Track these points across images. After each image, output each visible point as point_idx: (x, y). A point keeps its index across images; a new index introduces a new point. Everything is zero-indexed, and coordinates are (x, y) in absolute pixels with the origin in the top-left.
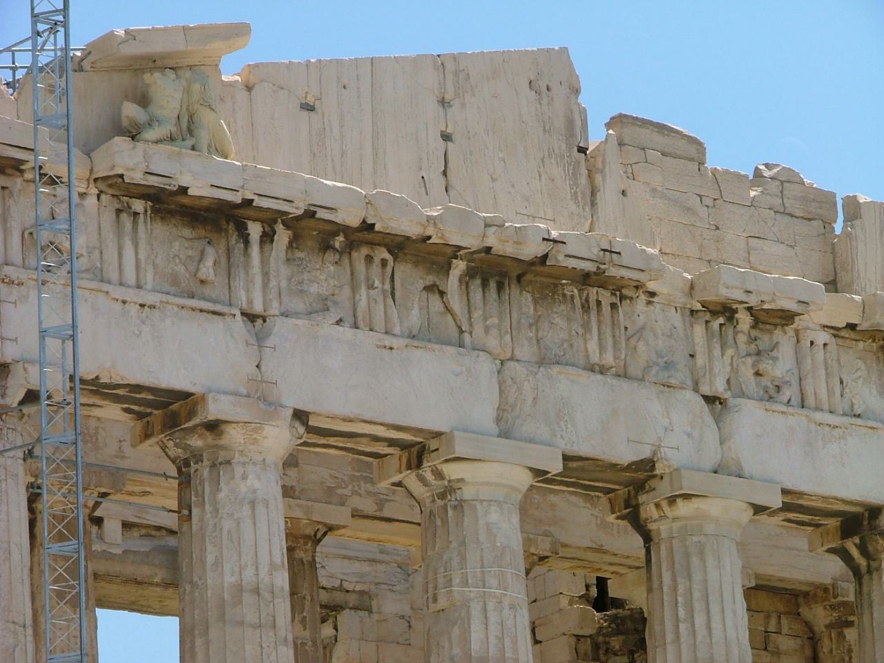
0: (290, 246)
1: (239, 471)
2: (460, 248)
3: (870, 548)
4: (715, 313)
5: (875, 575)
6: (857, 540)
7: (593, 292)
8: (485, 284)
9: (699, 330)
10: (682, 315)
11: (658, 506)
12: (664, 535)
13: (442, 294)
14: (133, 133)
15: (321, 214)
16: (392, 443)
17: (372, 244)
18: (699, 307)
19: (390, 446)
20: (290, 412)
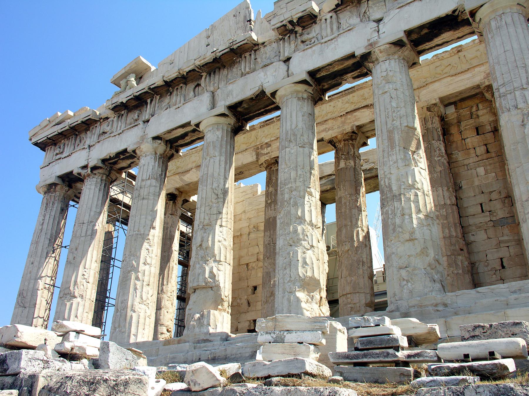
2: (194, 70)
4: (285, 35)
15: (152, 87)
18: (281, 37)
20: (151, 139)
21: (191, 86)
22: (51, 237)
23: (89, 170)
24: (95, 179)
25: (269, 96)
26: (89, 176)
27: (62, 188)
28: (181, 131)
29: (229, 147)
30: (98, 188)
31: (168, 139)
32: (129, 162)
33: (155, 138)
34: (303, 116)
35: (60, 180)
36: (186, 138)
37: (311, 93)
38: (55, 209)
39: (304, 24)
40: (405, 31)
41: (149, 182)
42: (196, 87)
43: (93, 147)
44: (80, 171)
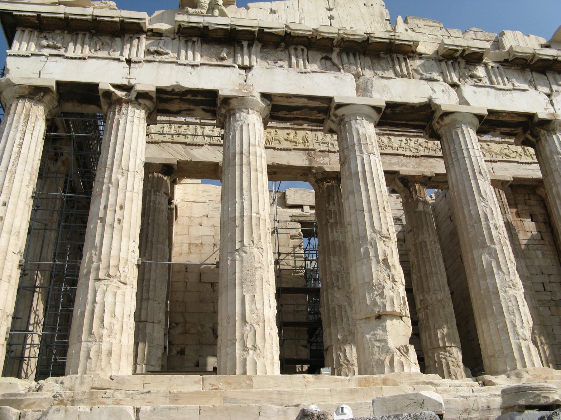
0: (263, 48)
1: (238, 115)
2: (332, 39)
3: (535, 133)
4: (449, 59)
5: (539, 142)
6: (529, 132)
7: (395, 55)
8: (348, 55)
9: (443, 64)
10: (436, 61)
11: (438, 123)
12: (443, 133)
13: (330, 59)
14: (187, 13)
15: (266, 30)
16: (319, 110)
17: (297, 44)
18: (441, 58)
19: (319, 113)
23: (133, 95)
26: (128, 102)
28: (304, 102)
32: (185, 106)
33: (265, 96)
36: (295, 112)
42: (322, 59)
43: (137, 65)
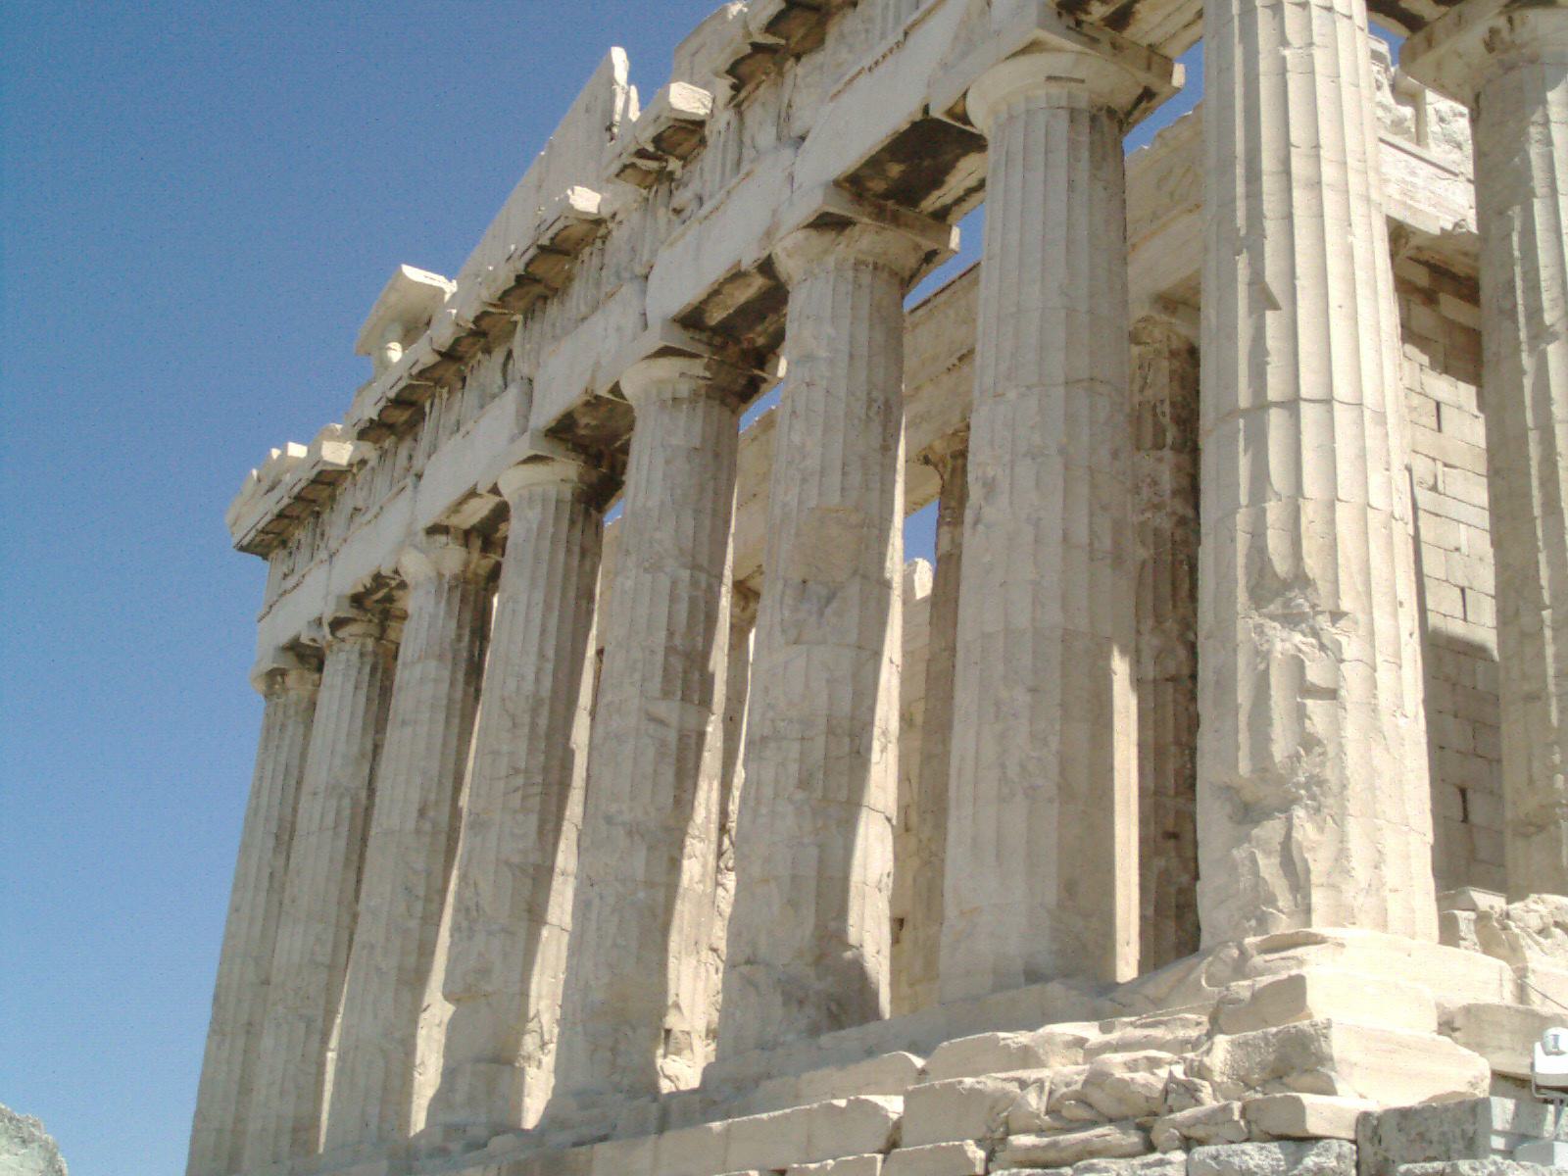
2: (484, 314)
15: (415, 371)
20: (422, 536)
21: (499, 355)
22: (279, 827)
24: (343, 656)
25: (610, 396)
27: (301, 678)
29: (561, 556)
30: (353, 679)
31: (467, 525)
33: (434, 530)
34: (667, 462)
35: (291, 655)
37: (705, 378)
38: (287, 741)
39: (679, 151)
40: (837, 184)
41: (419, 667)
44: (313, 634)
